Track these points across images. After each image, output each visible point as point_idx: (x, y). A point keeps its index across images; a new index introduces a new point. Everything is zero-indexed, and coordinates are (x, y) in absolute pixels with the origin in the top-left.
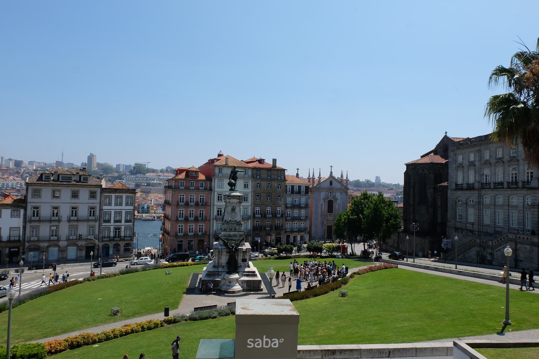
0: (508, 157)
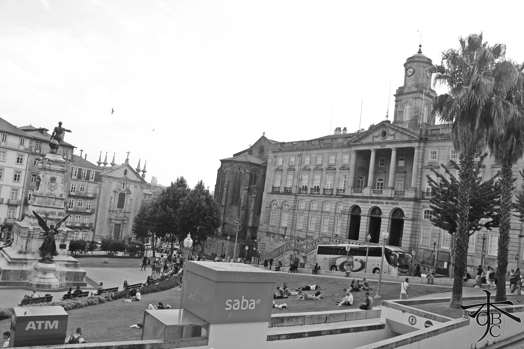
0: (327, 165)
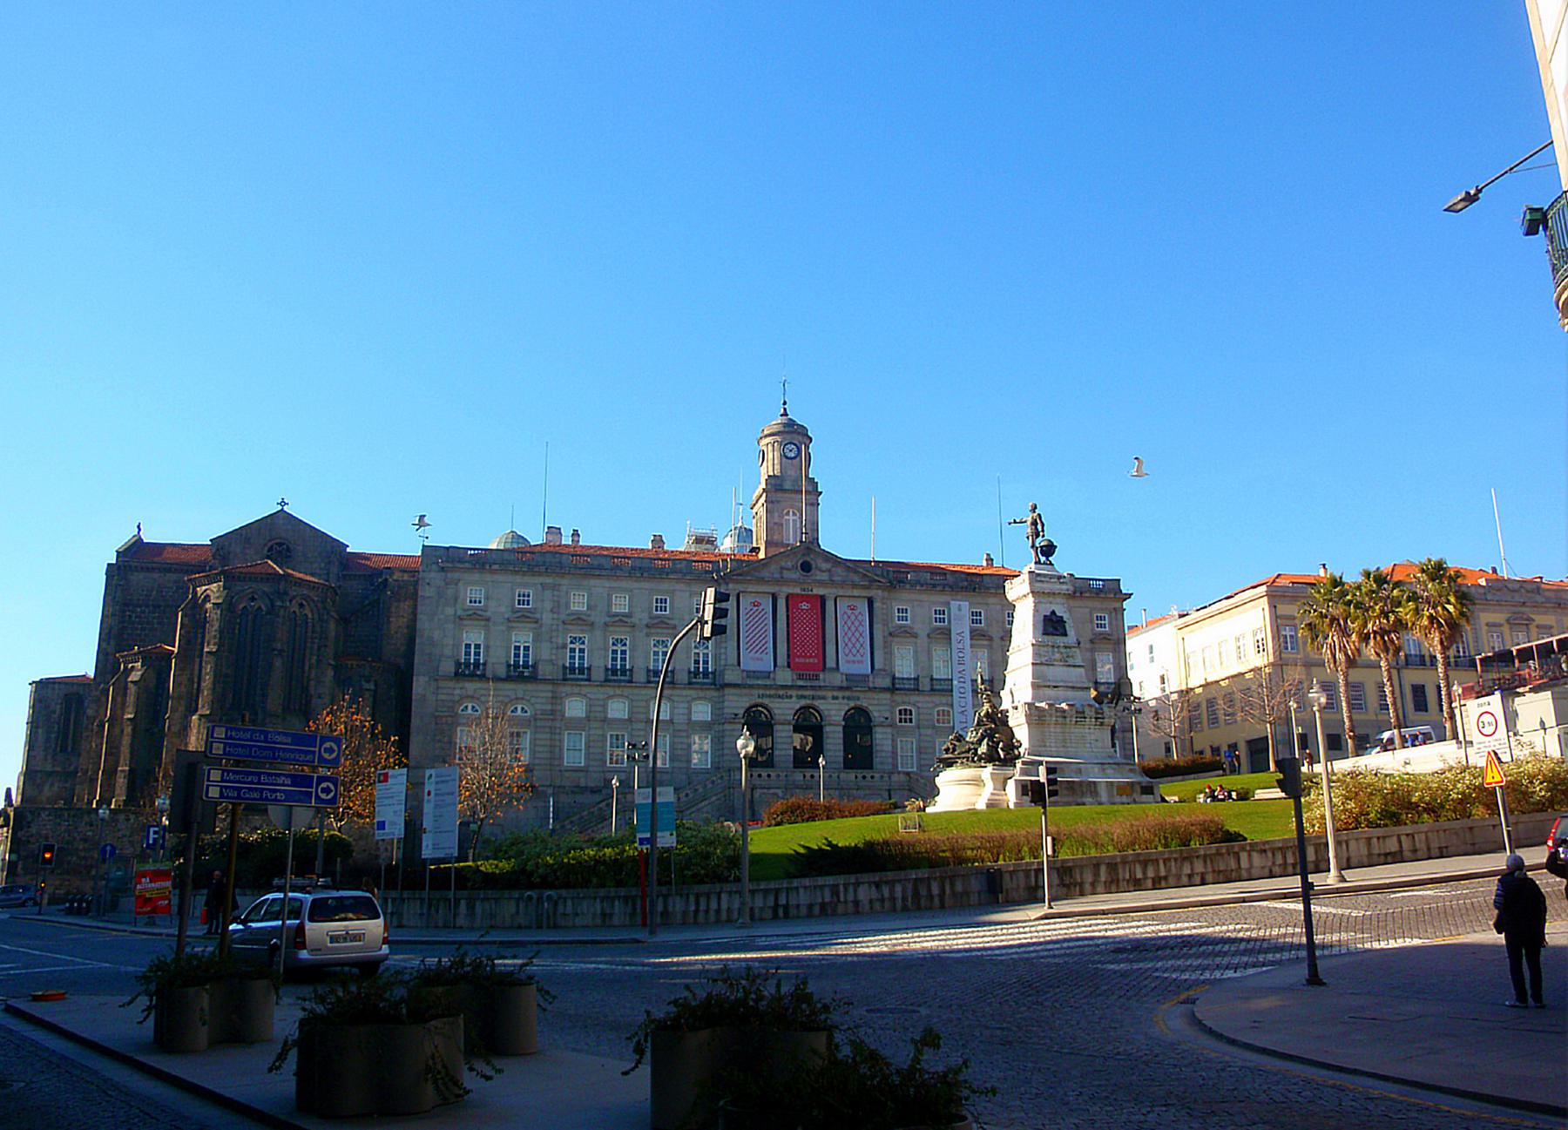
0: (646, 615)
